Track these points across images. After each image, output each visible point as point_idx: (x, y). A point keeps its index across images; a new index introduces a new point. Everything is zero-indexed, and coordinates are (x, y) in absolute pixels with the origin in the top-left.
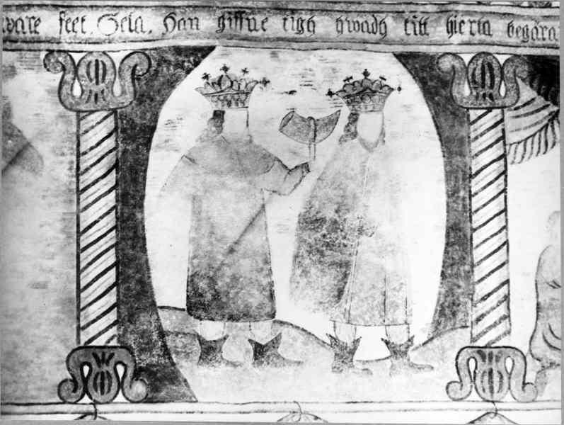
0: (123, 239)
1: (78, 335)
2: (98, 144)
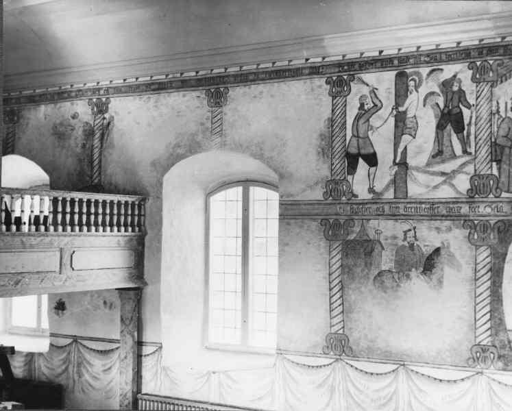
0: (494, 300)
1: (475, 340)
2: (484, 259)
